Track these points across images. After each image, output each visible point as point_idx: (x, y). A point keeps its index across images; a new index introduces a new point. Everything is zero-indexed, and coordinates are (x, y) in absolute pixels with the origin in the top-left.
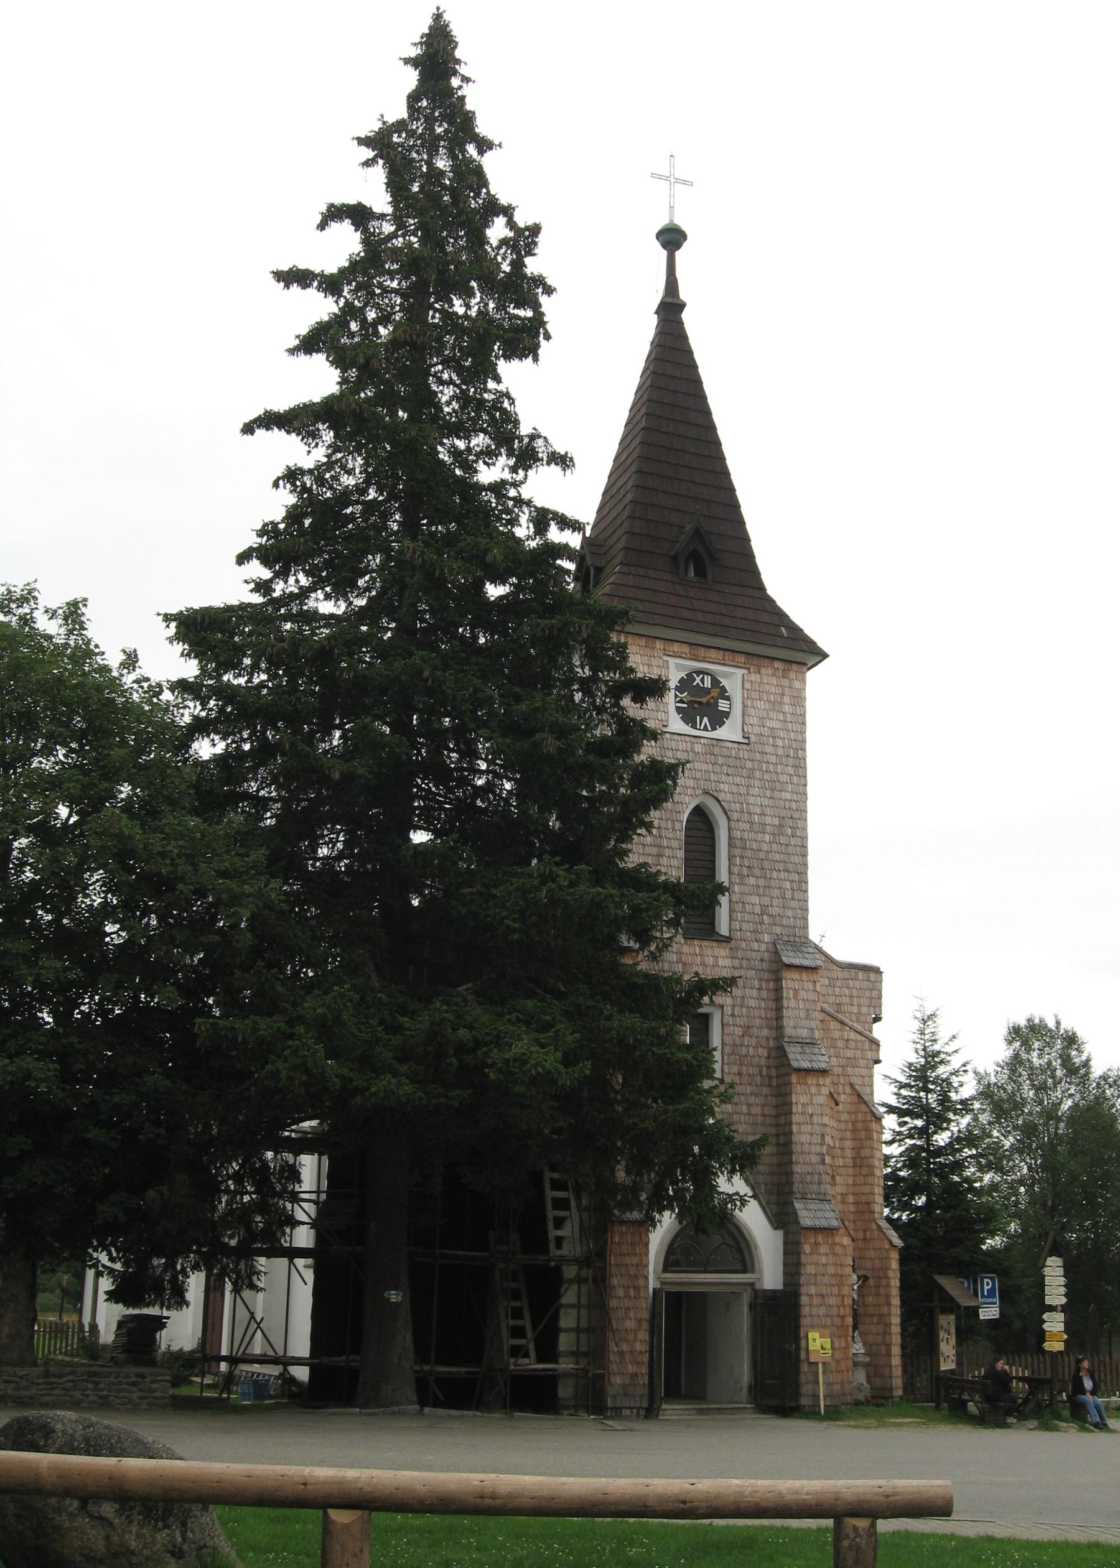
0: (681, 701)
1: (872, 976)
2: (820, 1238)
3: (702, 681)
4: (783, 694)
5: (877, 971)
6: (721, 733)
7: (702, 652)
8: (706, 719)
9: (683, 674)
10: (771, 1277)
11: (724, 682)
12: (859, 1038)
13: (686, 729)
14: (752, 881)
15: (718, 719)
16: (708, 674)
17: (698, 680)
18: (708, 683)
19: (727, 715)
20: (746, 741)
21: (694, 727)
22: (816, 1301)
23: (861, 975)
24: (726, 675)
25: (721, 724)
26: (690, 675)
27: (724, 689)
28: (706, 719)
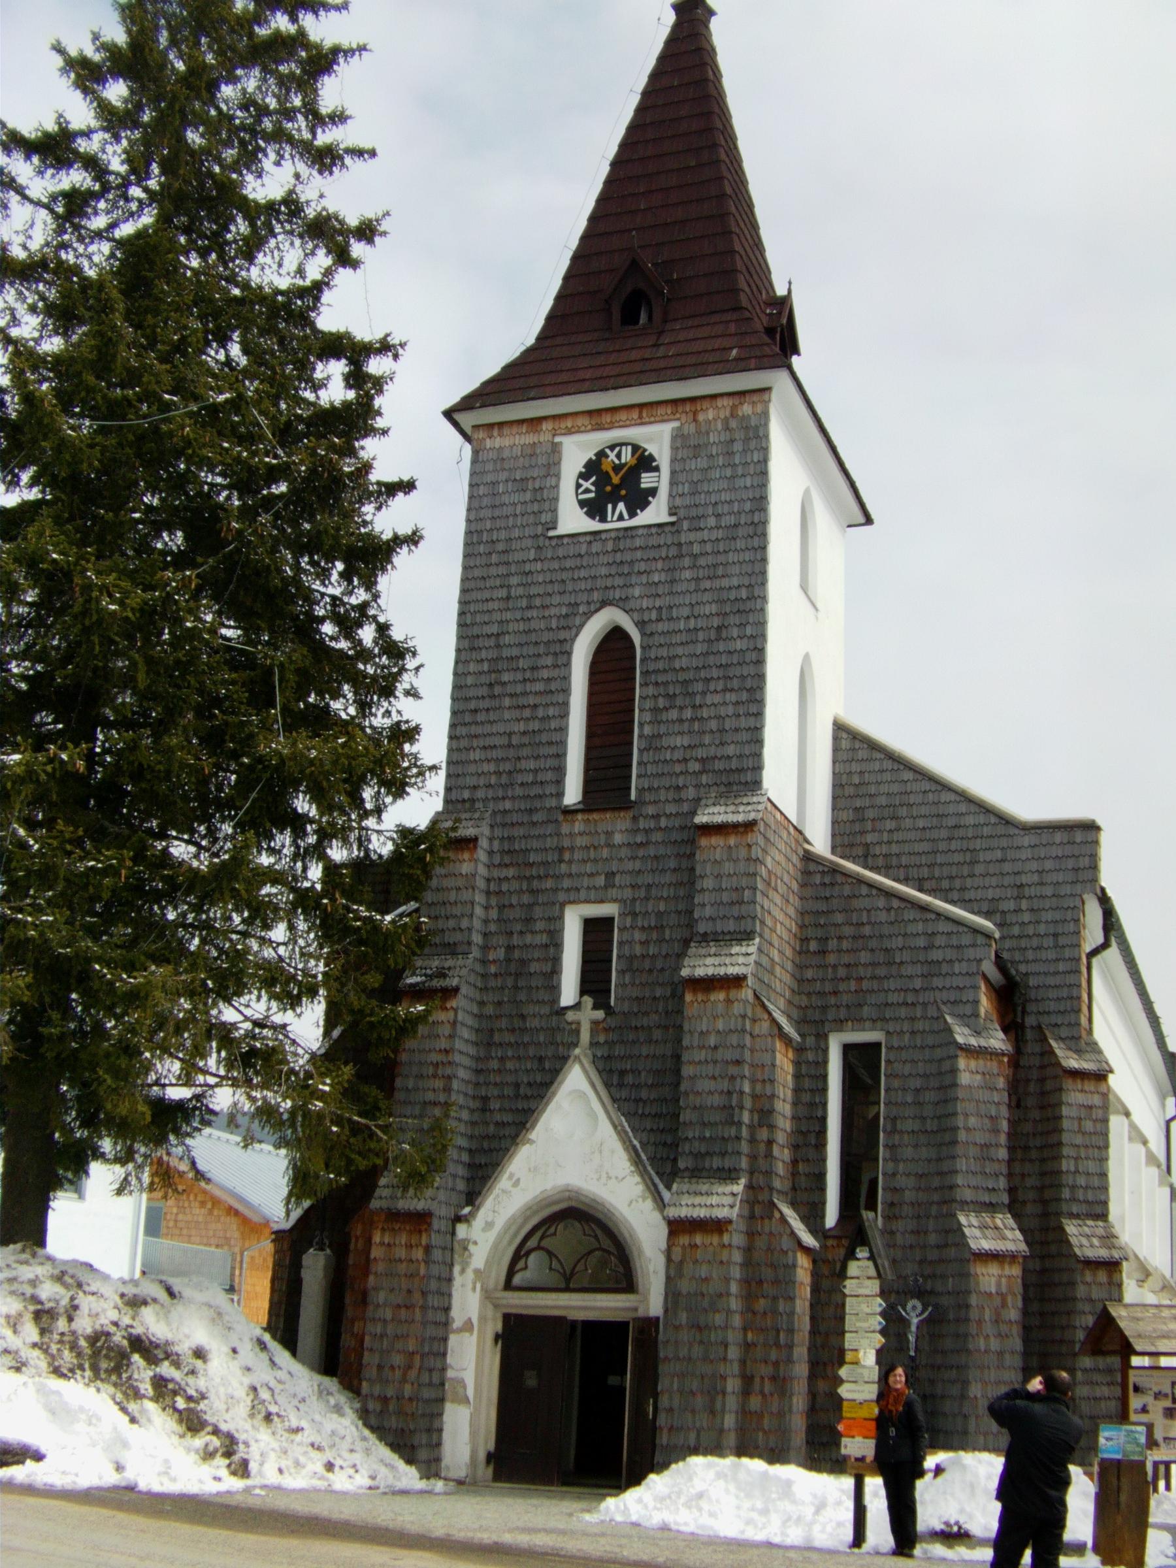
0: (587, 491)
1: (1079, 836)
2: (698, 1239)
3: (619, 456)
4: (732, 441)
5: (1091, 828)
6: (645, 517)
7: (607, 418)
8: (621, 506)
9: (591, 455)
10: (653, 1302)
11: (651, 449)
12: (950, 927)
13: (595, 525)
14: (673, 714)
15: (639, 500)
16: (626, 444)
17: (612, 456)
18: (627, 455)
19: (653, 492)
20: (673, 519)
21: (603, 519)
22: (685, 1336)
23: (1058, 837)
24: (650, 440)
25: (644, 505)
26: (601, 454)
27: (651, 458)
28: (621, 506)
